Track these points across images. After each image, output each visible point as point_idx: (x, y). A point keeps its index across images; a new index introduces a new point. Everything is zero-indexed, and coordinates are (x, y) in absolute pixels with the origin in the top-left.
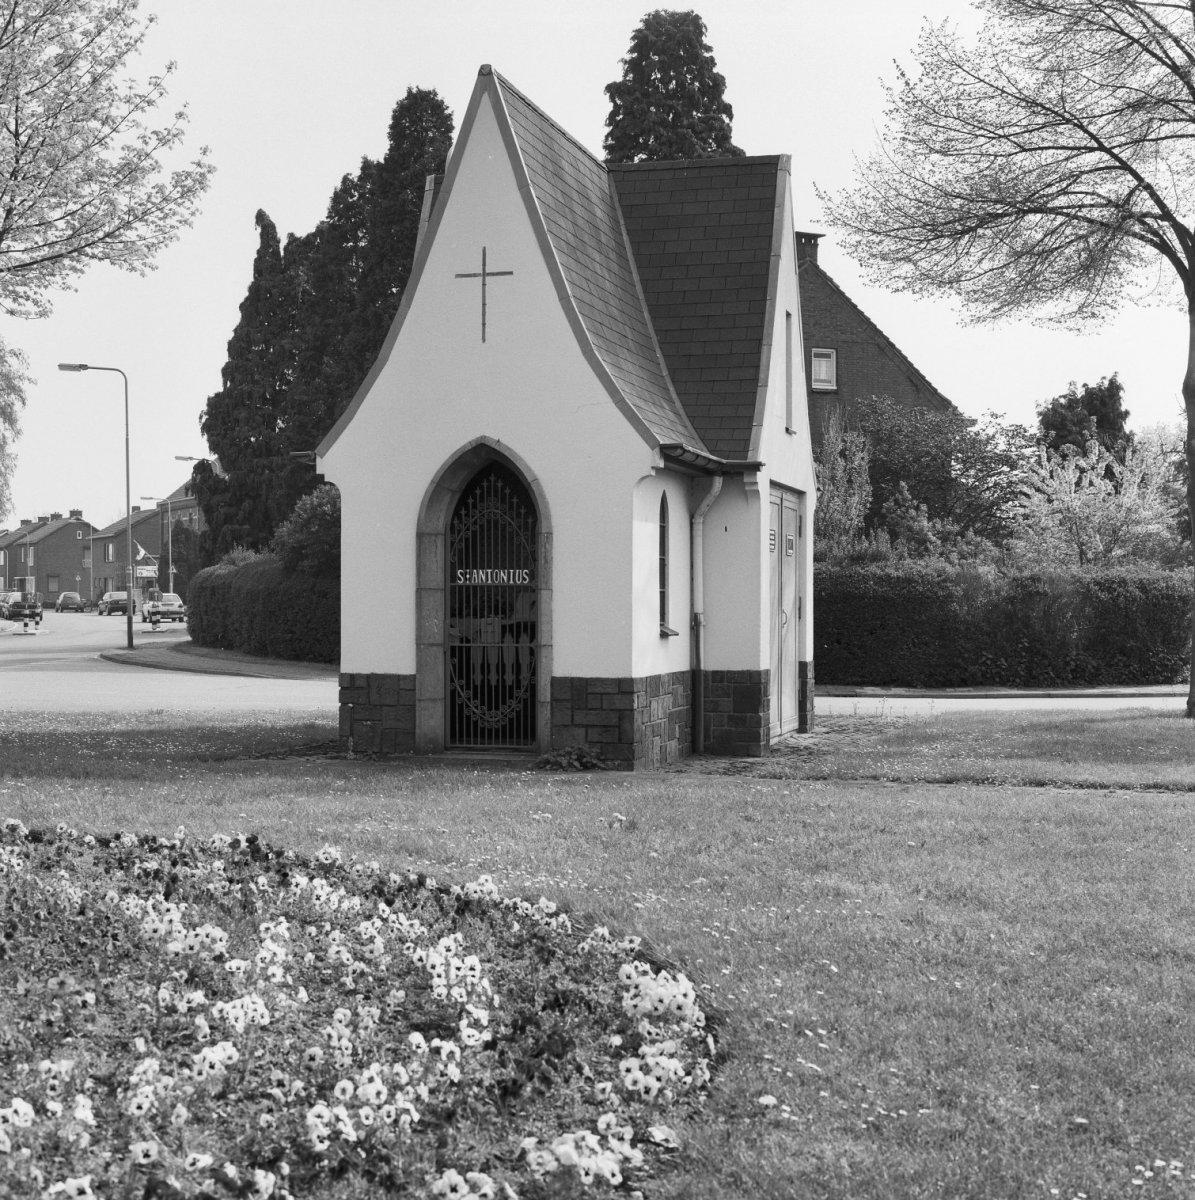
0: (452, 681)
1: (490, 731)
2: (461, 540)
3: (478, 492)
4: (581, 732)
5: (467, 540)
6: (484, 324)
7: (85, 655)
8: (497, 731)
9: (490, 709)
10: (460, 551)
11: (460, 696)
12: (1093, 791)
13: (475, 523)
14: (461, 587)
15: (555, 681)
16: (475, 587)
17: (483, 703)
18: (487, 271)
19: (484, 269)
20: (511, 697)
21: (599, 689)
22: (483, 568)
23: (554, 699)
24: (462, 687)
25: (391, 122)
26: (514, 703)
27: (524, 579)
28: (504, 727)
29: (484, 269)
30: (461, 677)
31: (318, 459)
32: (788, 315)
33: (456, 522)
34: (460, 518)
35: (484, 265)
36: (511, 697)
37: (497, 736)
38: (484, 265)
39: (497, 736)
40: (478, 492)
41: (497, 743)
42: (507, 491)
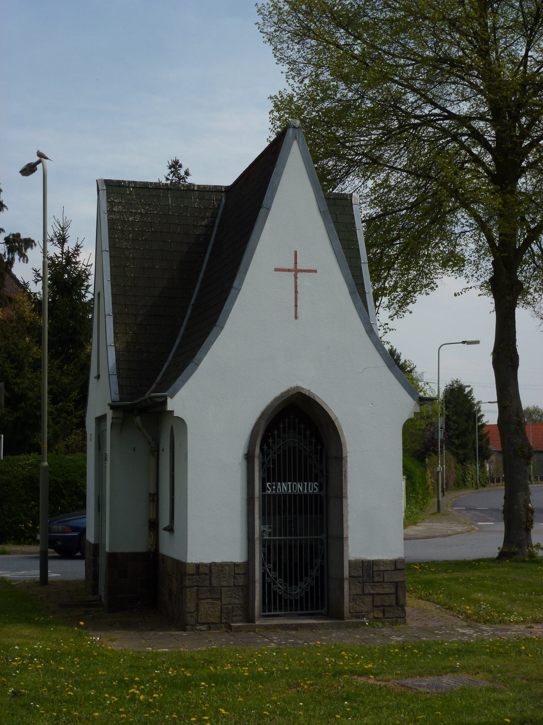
0: (263, 565)
1: (291, 601)
2: (269, 461)
3: (281, 426)
4: (369, 599)
5: (274, 461)
6: (296, 306)
7: (28, 555)
8: (296, 601)
9: (291, 585)
10: (269, 469)
11: (268, 576)
12: (453, 617)
13: (279, 448)
14: (269, 495)
15: (350, 562)
16: (279, 495)
17: (285, 581)
18: (298, 268)
19: (296, 266)
20: (306, 575)
21: (382, 568)
22: (285, 481)
23: (351, 576)
24: (270, 570)
25: (15, 233)
26: (309, 580)
27: (315, 490)
28: (301, 598)
29: (296, 266)
30: (269, 562)
31: (169, 400)
32: (98, 377)
33: (265, 447)
34: (268, 444)
35: (296, 263)
36: (306, 575)
37: (291, 605)
38: (296, 263)
39: (291, 605)
40: (281, 426)
41: (286, 610)
42: (302, 426)
